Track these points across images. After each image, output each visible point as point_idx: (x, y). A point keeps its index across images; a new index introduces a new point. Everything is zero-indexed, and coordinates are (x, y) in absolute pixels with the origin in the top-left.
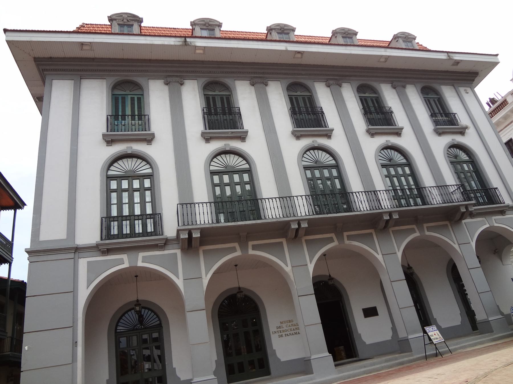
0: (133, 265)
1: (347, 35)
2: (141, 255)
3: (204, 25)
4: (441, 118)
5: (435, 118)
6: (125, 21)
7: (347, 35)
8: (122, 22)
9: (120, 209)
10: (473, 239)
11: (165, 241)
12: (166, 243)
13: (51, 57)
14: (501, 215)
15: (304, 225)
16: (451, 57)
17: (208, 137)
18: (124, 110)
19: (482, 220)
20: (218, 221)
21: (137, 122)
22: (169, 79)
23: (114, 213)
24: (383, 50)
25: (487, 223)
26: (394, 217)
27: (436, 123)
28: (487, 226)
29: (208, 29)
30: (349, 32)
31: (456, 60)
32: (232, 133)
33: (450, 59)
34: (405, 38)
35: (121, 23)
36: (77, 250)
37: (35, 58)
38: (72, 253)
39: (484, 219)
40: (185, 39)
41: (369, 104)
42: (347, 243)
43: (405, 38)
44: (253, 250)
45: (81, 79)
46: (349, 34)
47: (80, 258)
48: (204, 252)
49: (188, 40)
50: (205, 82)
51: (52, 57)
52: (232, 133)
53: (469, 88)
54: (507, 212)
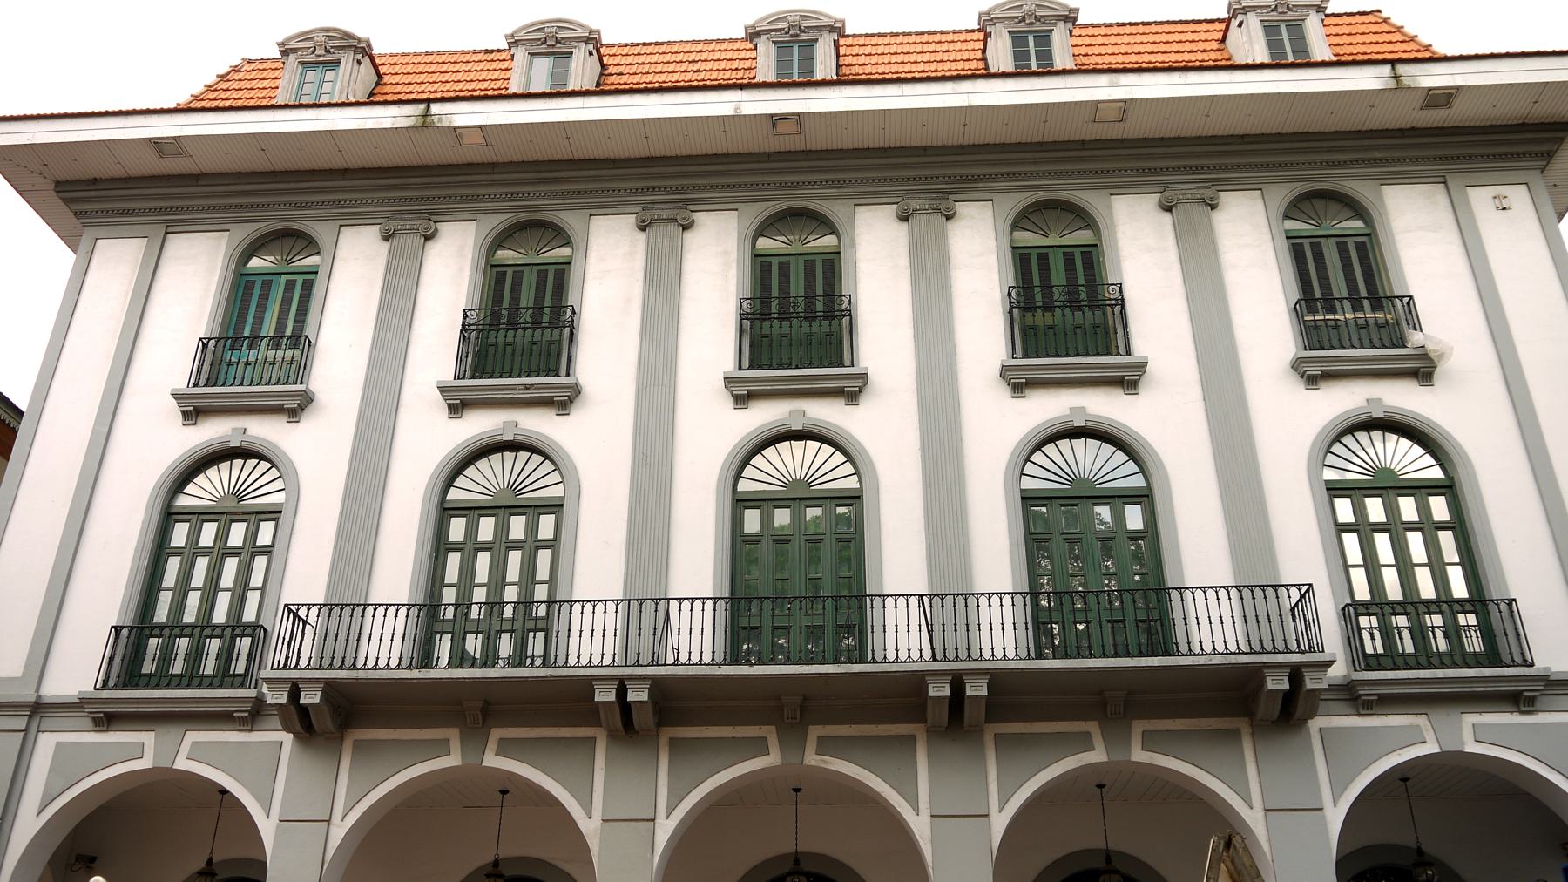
0: (165, 764)
1: (1031, 24)
2: (194, 736)
3: (542, 44)
4: (1350, 316)
5: (1322, 318)
6: (318, 52)
7: (1031, 24)
8: (313, 55)
9: (179, 605)
10: (1338, 799)
11: (251, 705)
12: (255, 714)
13: (95, 179)
14: (1512, 712)
15: (637, 695)
16: (1406, 81)
17: (455, 402)
18: (259, 320)
19: (1411, 726)
20: (425, 658)
21: (289, 353)
22: (393, 225)
23: (161, 615)
24: (1104, 79)
25: (1429, 735)
27: (1312, 335)
28: (1431, 748)
29: (553, 53)
30: (1041, 13)
31: (1430, 89)
32: (527, 387)
33: (1399, 87)
35: (311, 58)
36: (39, 710)
37: (58, 183)
38: (22, 717)
39: (1421, 721)
40: (428, 107)
41: (1053, 272)
42: (813, 763)
43: (1275, 9)
44: (497, 754)
45: (167, 233)
47: (43, 732)
48: (358, 745)
49: (436, 108)
50: (501, 228)
51: (98, 178)
52: (527, 388)
53: (1524, 187)
54: (1542, 702)
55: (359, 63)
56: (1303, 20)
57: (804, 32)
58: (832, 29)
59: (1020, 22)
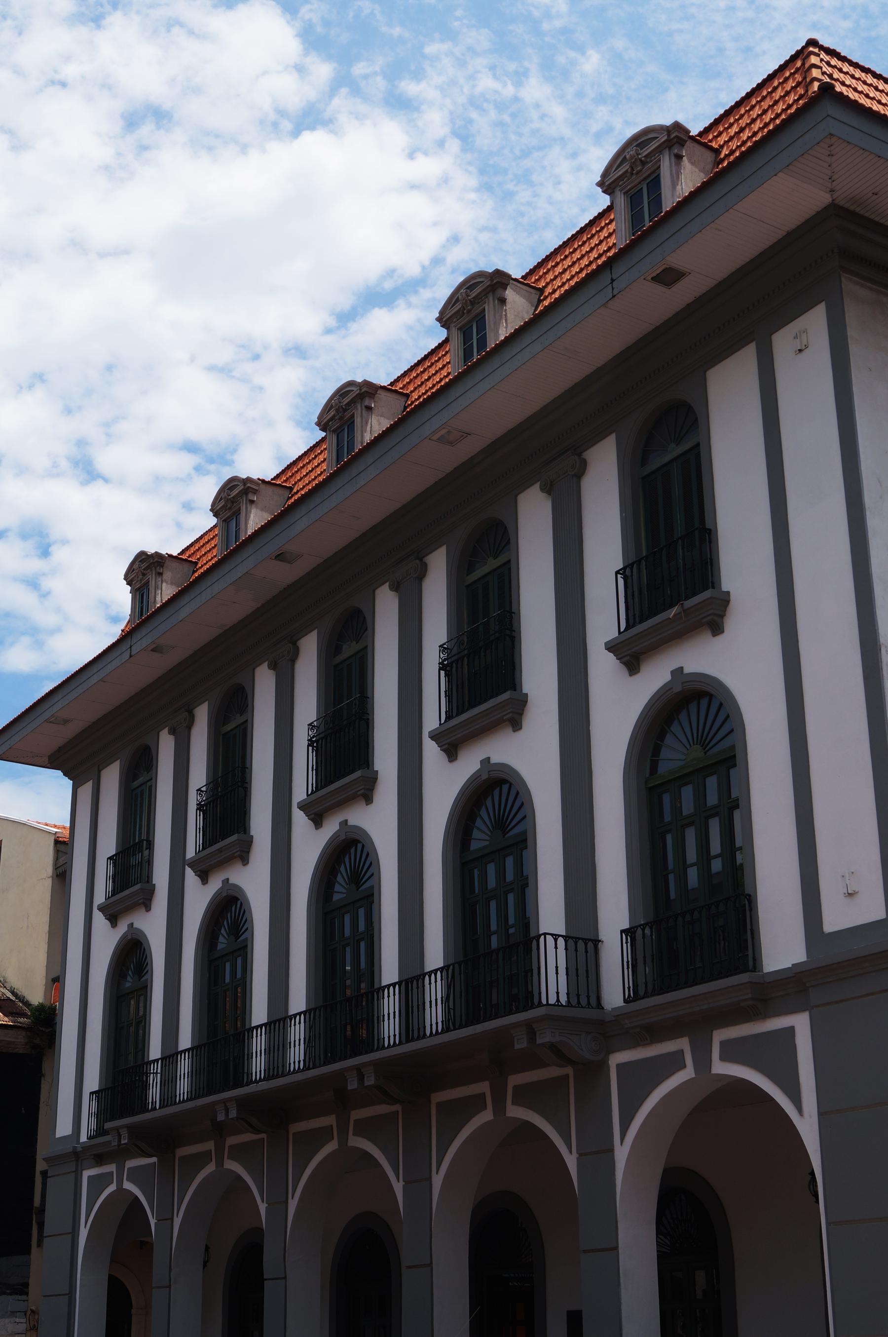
1: (469, 311)
26: (367, 1083)
30: (473, 294)
32: (220, 850)
34: (632, 174)
39: (683, 1044)
46: (473, 302)
52: (221, 852)
55: (160, 574)
56: (659, 167)
57: (345, 410)
58: (361, 396)
59: (464, 313)
